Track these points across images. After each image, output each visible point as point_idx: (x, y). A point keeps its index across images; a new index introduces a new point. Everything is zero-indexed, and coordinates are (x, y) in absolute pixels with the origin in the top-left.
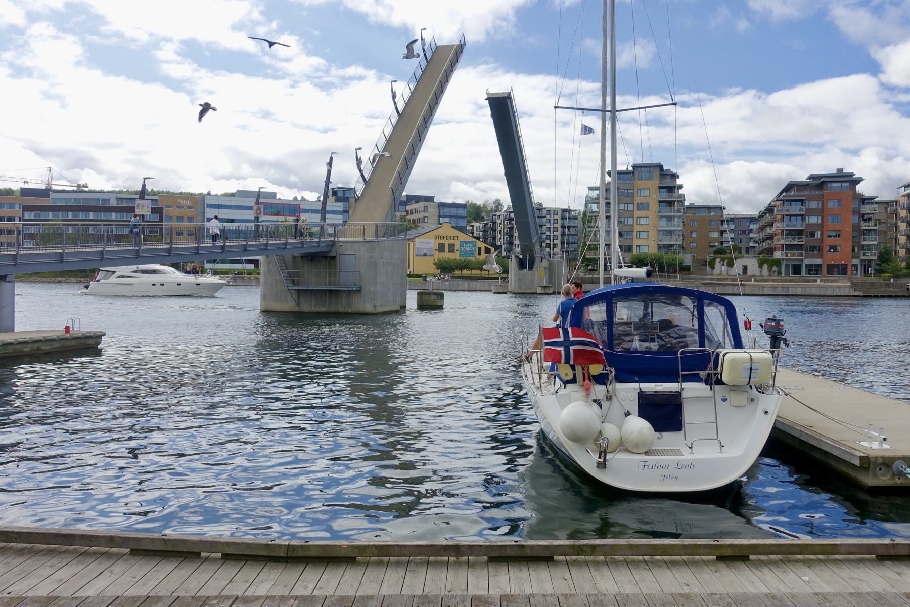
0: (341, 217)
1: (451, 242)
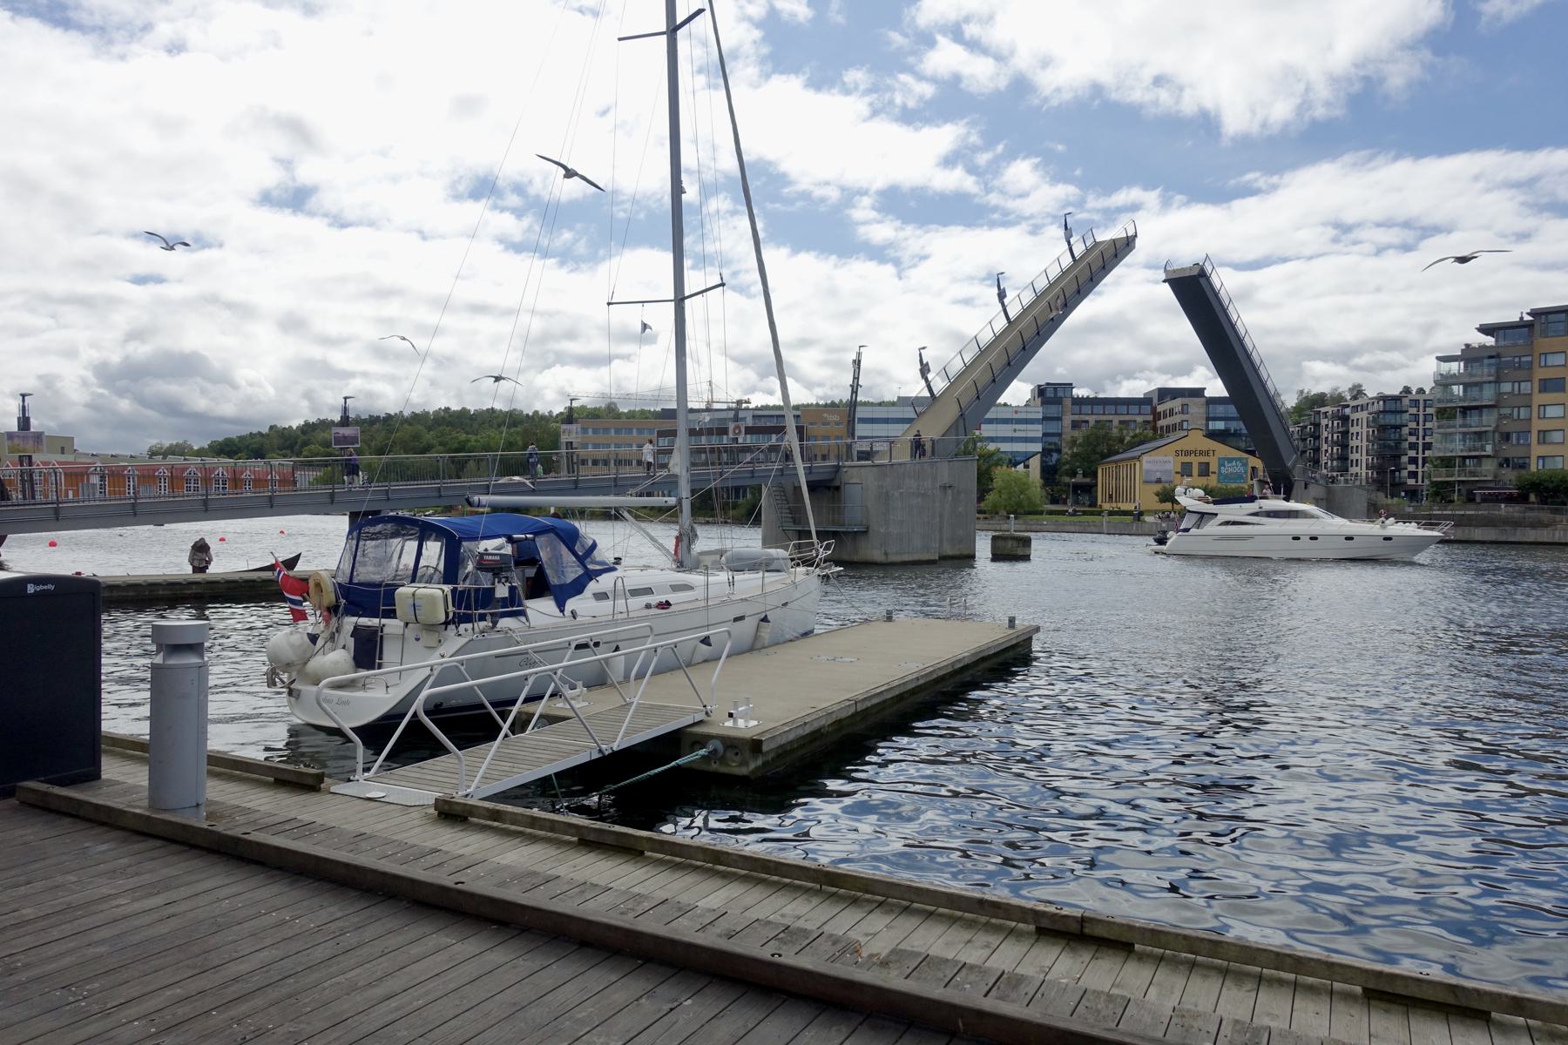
0: (1039, 427)
1: (1204, 459)
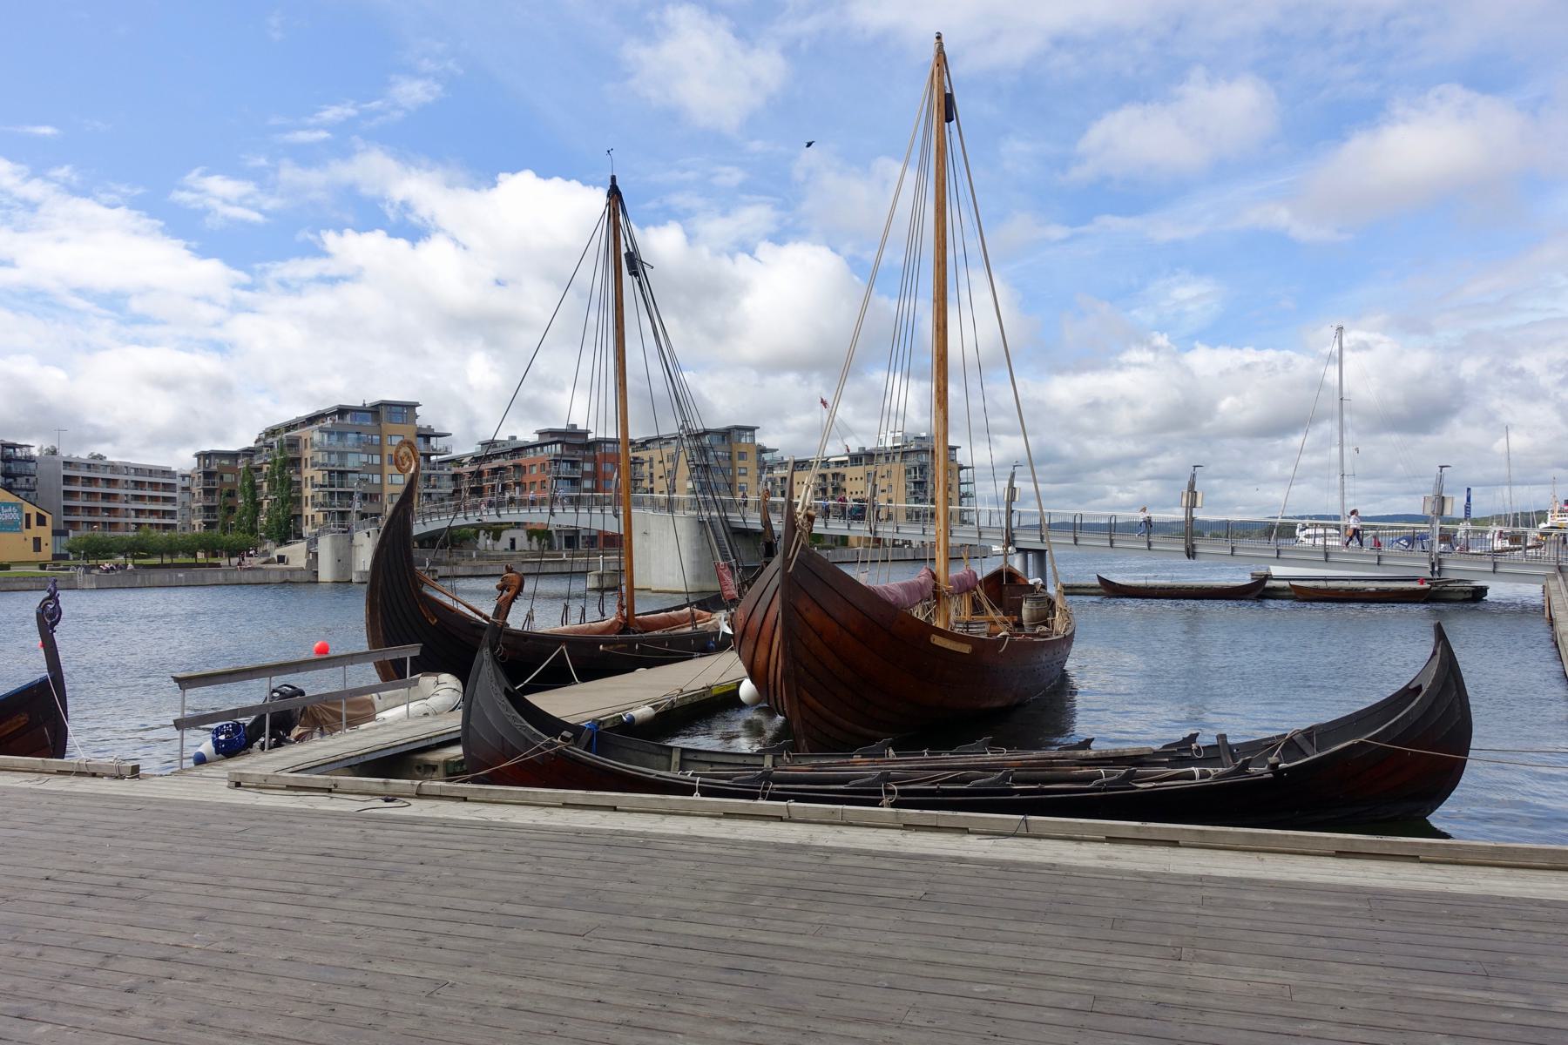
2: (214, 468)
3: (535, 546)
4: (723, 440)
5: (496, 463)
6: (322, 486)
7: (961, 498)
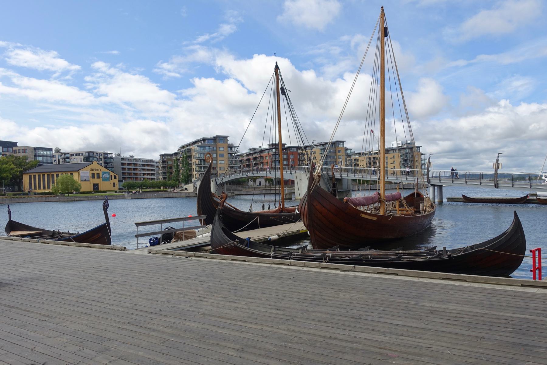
1: (98, 172)
2: (165, 159)
3: (267, 184)
4: (333, 146)
5: (254, 156)
6: (198, 165)
7: (422, 165)
